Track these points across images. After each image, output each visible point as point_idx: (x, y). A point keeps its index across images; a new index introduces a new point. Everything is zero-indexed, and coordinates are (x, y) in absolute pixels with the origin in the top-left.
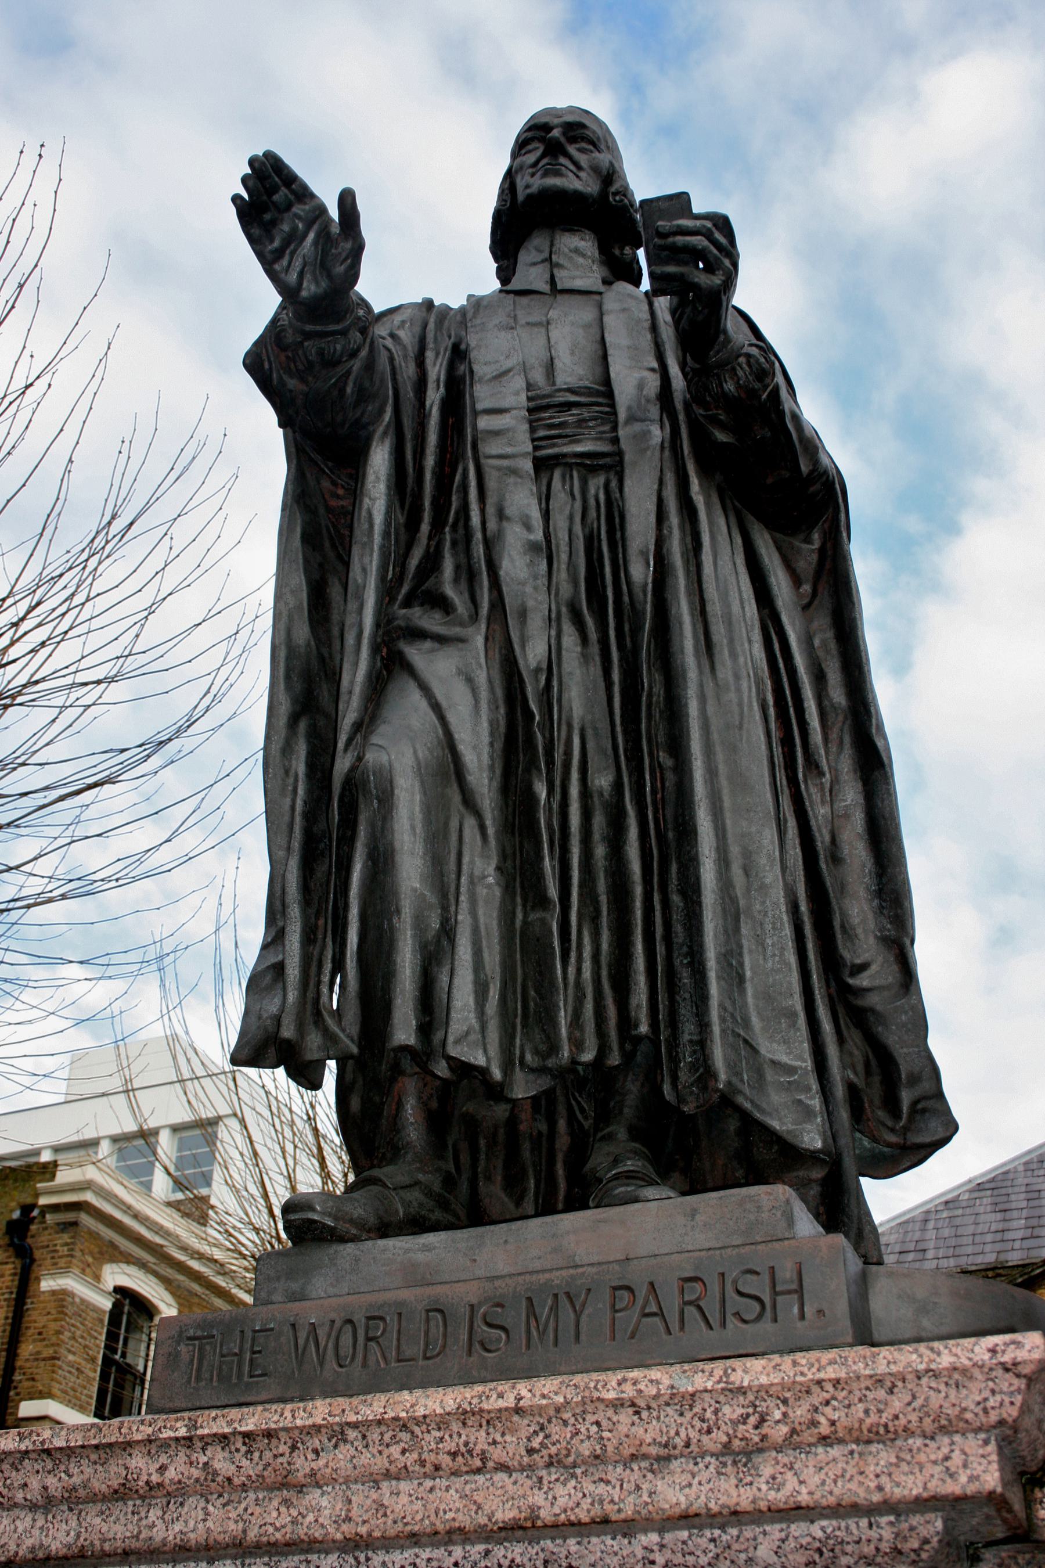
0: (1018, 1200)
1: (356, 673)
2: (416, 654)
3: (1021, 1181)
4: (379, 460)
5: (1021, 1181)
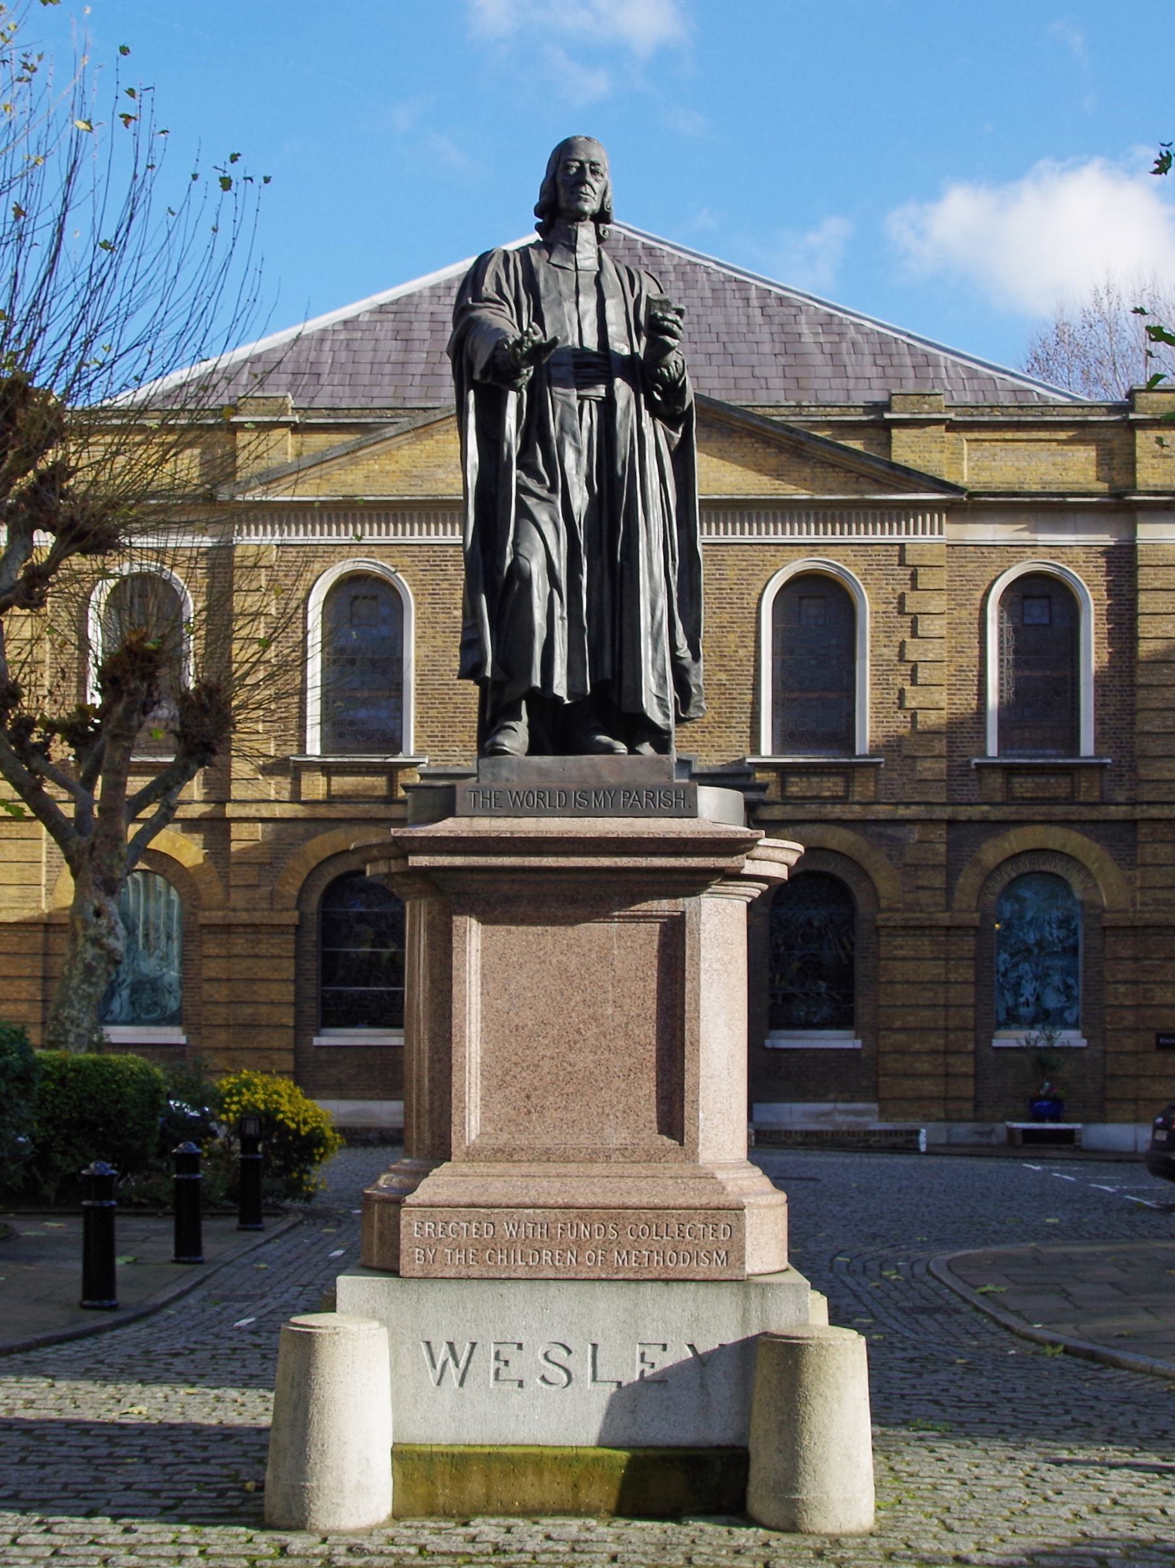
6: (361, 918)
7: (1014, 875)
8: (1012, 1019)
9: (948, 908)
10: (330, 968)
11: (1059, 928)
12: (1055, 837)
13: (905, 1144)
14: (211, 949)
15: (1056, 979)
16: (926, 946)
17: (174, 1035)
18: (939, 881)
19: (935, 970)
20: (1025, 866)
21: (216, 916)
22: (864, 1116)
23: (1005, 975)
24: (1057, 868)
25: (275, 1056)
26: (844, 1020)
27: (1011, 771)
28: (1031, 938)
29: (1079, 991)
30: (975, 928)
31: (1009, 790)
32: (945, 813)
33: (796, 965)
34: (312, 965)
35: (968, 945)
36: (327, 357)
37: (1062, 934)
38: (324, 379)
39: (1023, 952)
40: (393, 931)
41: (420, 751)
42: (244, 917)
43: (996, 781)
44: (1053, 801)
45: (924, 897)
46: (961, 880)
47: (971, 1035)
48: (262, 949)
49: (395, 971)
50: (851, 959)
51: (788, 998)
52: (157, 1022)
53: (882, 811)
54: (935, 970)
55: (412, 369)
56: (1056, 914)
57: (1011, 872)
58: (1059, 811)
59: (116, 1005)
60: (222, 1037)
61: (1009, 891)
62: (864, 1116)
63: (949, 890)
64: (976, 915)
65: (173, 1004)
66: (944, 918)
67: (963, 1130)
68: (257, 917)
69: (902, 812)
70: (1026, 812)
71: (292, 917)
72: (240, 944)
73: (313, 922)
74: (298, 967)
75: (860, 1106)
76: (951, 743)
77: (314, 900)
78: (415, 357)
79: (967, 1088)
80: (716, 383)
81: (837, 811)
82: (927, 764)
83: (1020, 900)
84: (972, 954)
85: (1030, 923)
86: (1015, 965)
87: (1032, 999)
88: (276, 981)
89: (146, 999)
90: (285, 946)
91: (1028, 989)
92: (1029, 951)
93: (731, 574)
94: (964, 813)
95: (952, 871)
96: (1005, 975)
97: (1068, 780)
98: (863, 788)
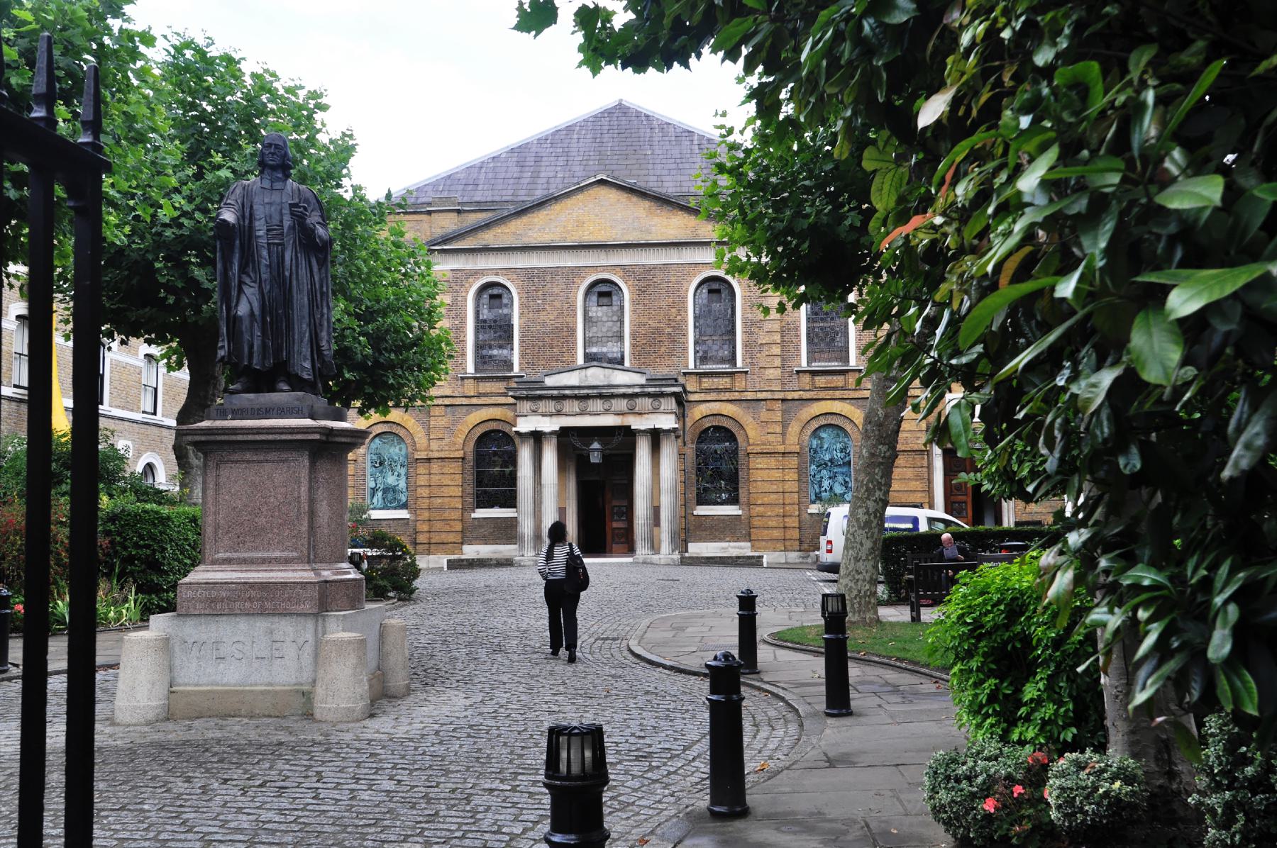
0: (530, 160)
1: (234, 293)
2: (246, 289)
3: (534, 149)
4: (238, 242)
5: (534, 149)
6: (495, 453)
8: (818, 498)
9: (784, 443)
10: (480, 480)
12: (837, 407)
13: (755, 562)
14: (422, 469)
15: (840, 479)
16: (772, 462)
17: (403, 514)
18: (778, 429)
19: (777, 474)
20: (823, 421)
21: (423, 455)
22: (741, 548)
24: (832, 420)
25: (452, 523)
26: (734, 501)
27: (814, 373)
28: (827, 457)
29: (852, 484)
31: (814, 383)
32: (781, 395)
33: (709, 472)
34: (470, 478)
35: (794, 461)
36: (482, 176)
38: (480, 187)
39: (822, 465)
40: (512, 459)
41: (521, 370)
42: (436, 455)
43: (806, 378)
44: (835, 388)
45: (771, 438)
47: (796, 507)
48: (446, 470)
49: (512, 479)
50: (737, 470)
51: (706, 490)
52: (395, 508)
53: (750, 396)
54: (777, 474)
55: (522, 181)
56: (839, 446)
57: (815, 424)
58: (838, 394)
59: (375, 500)
60: (426, 515)
61: (815, 433)
62: (741, 548)
63: (783, 434)
65: (404, 499)
66: (781, 449)
67: (793, 556)
68: (442, 455)
69: (760, 396)
70: (822, 395)
71: (460, 454)
72: (435, 467)
73: (470, 457)
74: (463, 478)
75: (742, 544)
76: (783, 360)
77: (471, 446)
78: (525, 175)
79: (795, 534)
80: (671, 184)
81: (727, 396)
82: (771, 371)
83: (821, 439)
88: (452, 485)
89: (390, 496)
90: (456, 467)
91: (826, 484)
93: (673, 279)
94: (790, 396)
95: (785, 425)
98: (740, 383)
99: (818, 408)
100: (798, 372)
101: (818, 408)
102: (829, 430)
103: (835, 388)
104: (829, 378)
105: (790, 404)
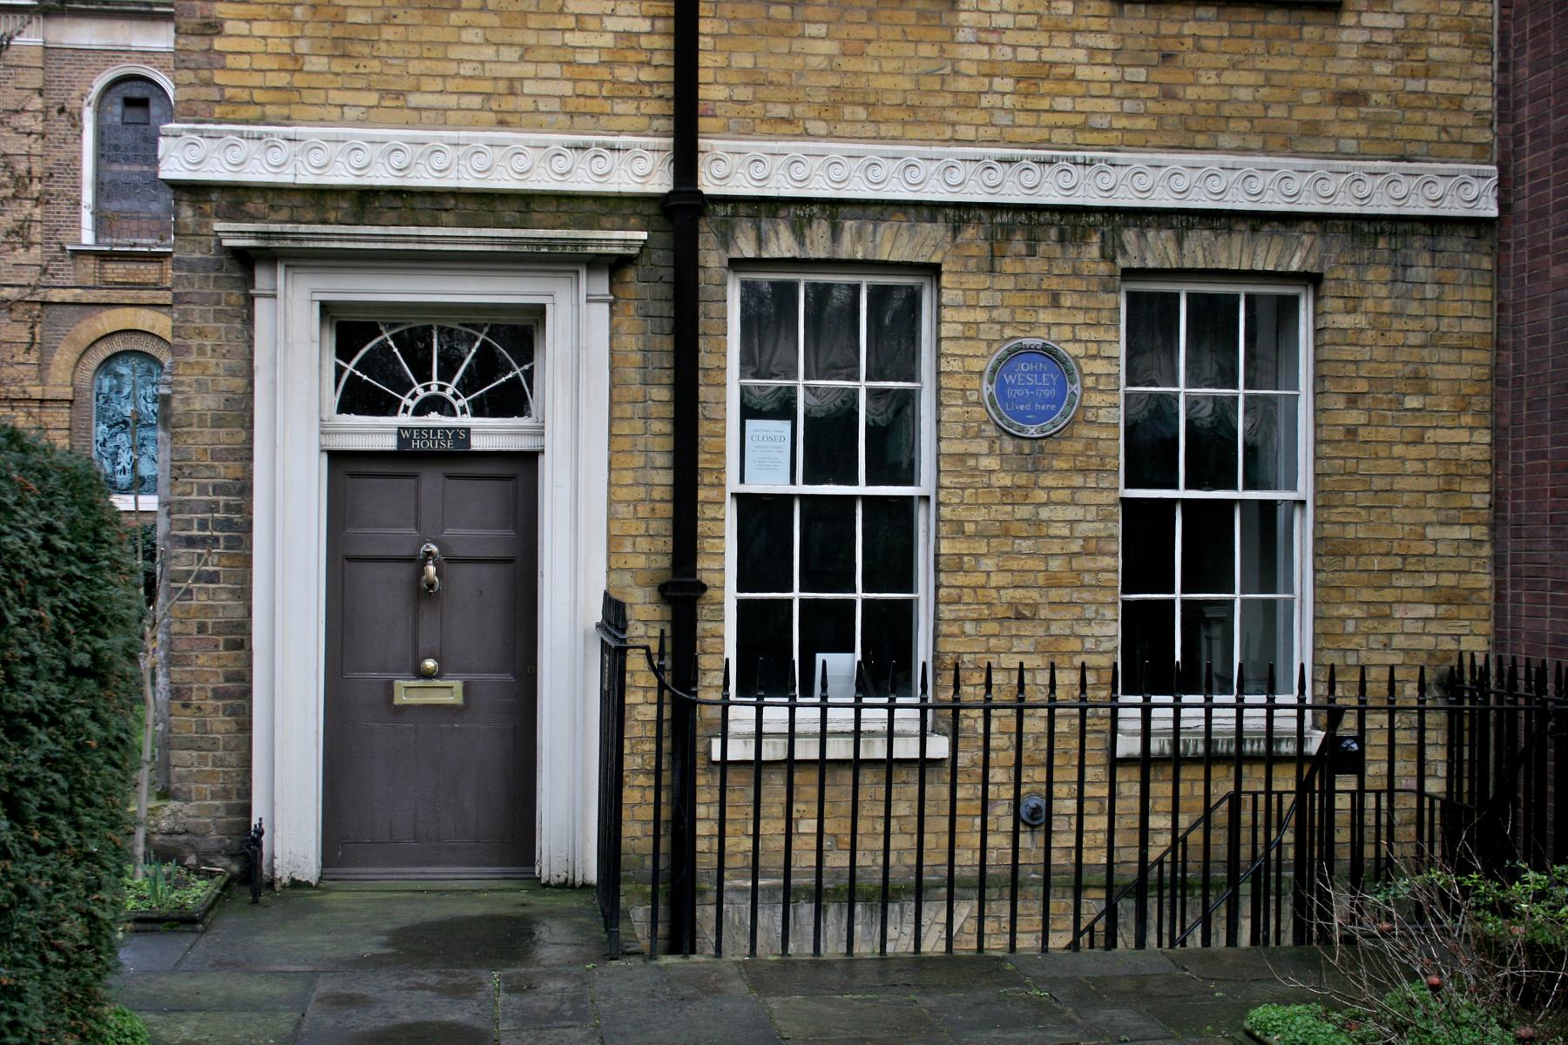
7: (108, 353)
9: (43, 382)
11: (155, 402)
20: (119, 345)
23: (103, 445)
27: (104, 257)
28: (128, 410)
30: (71, 402)
37: (156, 407)
43: (91, 264)
44: (142, 286)
46: (57, 357)
57: (105, 350)
58: (146, 296)
64: (70, 390)
66: (36, 392)
70: (115, 296)
83: (118, 376)
84: (66, 425)
85: (127, 397)
86: (114, 436)
87: (128, 467)
91: (125, 459)
92: (125, 422)
94: (56, 296)
96: (103, 445)
97: (156, 266)
99: (110, 321)
100: (75, 253)
101: (110, 321)
102: (134, 361)
103: (142, 286)
104: (133, 266)
105: (58, 311)
